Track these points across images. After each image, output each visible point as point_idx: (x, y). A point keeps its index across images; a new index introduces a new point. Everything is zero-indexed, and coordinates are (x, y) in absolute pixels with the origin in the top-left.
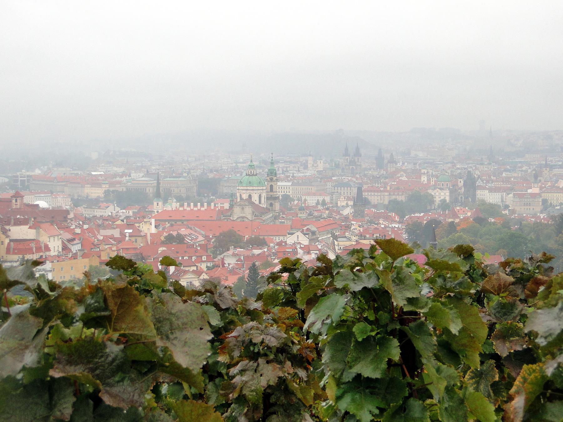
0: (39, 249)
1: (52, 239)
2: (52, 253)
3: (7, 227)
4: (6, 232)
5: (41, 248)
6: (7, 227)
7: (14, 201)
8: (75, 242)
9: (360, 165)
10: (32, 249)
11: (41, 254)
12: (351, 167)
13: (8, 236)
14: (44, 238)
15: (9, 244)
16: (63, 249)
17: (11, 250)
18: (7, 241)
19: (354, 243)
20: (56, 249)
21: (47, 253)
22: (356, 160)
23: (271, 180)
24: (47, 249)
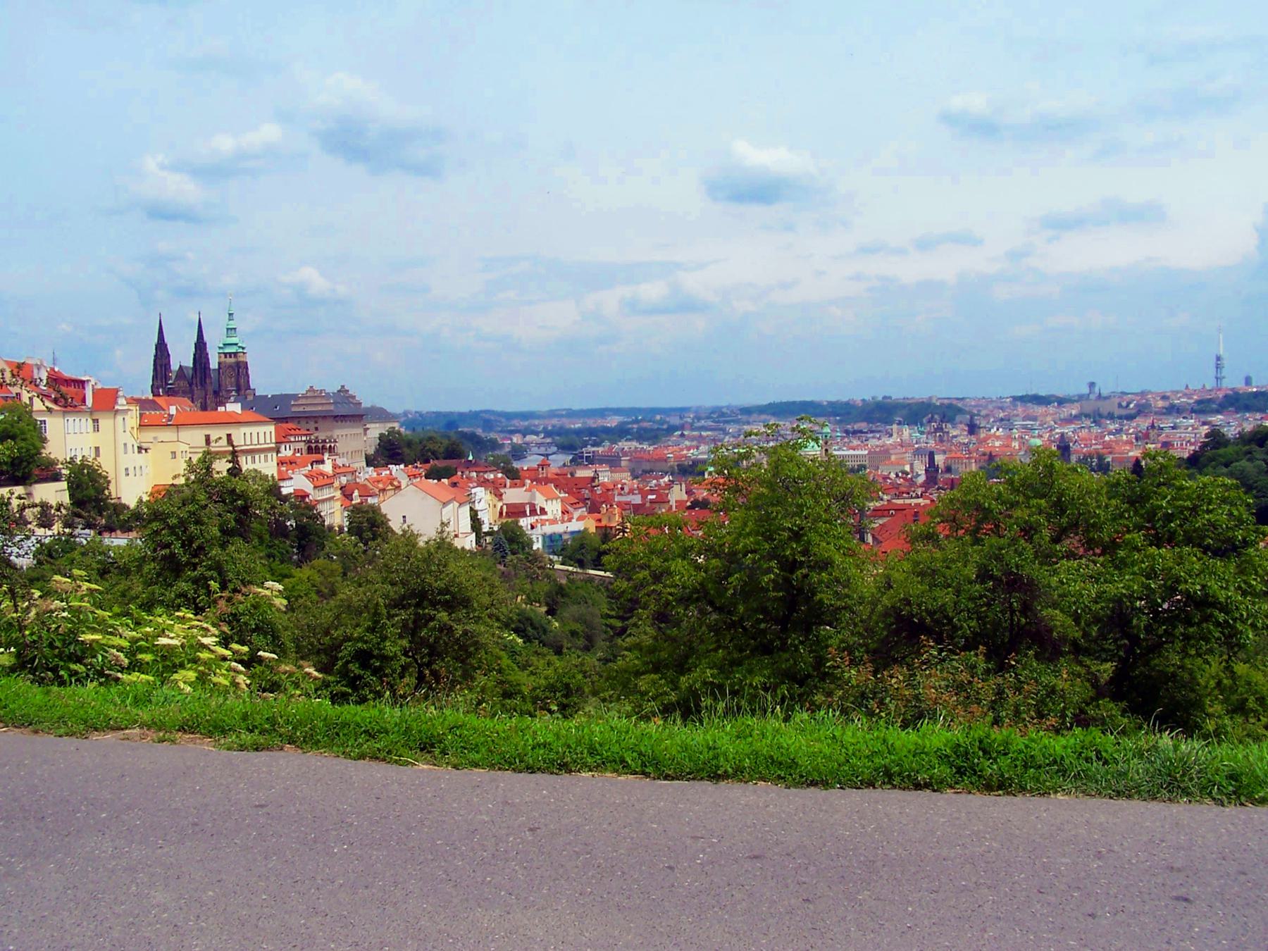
0: (533, 512)
1: (549, 502)
2: (549, 516)
3: (502, 491)
4: (501, 495)
5: (536, 510)
6: (502, 491)
7: (540, 469)
8: (577, 506)
9: (948, 432)
10: (525, 511)
11: (536, 517)
12: (938, 434)
13: (501, 499)
14: (540, 501)
15: (502, 508)
16: (563, 512)
17: (504, 514)
18: (500, 504)
19: (886, 503)
20: (555, 512)
21: (544, 517)
22: (944, 426)
23: (826, 443)
24: (543, 511)
